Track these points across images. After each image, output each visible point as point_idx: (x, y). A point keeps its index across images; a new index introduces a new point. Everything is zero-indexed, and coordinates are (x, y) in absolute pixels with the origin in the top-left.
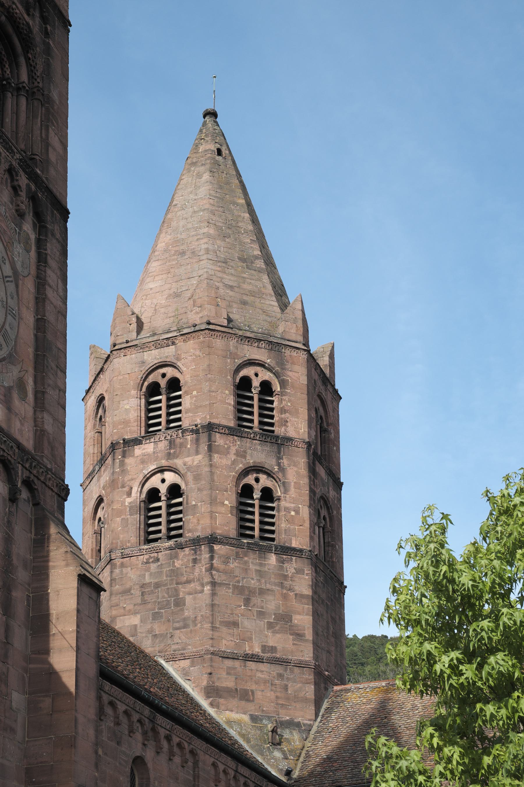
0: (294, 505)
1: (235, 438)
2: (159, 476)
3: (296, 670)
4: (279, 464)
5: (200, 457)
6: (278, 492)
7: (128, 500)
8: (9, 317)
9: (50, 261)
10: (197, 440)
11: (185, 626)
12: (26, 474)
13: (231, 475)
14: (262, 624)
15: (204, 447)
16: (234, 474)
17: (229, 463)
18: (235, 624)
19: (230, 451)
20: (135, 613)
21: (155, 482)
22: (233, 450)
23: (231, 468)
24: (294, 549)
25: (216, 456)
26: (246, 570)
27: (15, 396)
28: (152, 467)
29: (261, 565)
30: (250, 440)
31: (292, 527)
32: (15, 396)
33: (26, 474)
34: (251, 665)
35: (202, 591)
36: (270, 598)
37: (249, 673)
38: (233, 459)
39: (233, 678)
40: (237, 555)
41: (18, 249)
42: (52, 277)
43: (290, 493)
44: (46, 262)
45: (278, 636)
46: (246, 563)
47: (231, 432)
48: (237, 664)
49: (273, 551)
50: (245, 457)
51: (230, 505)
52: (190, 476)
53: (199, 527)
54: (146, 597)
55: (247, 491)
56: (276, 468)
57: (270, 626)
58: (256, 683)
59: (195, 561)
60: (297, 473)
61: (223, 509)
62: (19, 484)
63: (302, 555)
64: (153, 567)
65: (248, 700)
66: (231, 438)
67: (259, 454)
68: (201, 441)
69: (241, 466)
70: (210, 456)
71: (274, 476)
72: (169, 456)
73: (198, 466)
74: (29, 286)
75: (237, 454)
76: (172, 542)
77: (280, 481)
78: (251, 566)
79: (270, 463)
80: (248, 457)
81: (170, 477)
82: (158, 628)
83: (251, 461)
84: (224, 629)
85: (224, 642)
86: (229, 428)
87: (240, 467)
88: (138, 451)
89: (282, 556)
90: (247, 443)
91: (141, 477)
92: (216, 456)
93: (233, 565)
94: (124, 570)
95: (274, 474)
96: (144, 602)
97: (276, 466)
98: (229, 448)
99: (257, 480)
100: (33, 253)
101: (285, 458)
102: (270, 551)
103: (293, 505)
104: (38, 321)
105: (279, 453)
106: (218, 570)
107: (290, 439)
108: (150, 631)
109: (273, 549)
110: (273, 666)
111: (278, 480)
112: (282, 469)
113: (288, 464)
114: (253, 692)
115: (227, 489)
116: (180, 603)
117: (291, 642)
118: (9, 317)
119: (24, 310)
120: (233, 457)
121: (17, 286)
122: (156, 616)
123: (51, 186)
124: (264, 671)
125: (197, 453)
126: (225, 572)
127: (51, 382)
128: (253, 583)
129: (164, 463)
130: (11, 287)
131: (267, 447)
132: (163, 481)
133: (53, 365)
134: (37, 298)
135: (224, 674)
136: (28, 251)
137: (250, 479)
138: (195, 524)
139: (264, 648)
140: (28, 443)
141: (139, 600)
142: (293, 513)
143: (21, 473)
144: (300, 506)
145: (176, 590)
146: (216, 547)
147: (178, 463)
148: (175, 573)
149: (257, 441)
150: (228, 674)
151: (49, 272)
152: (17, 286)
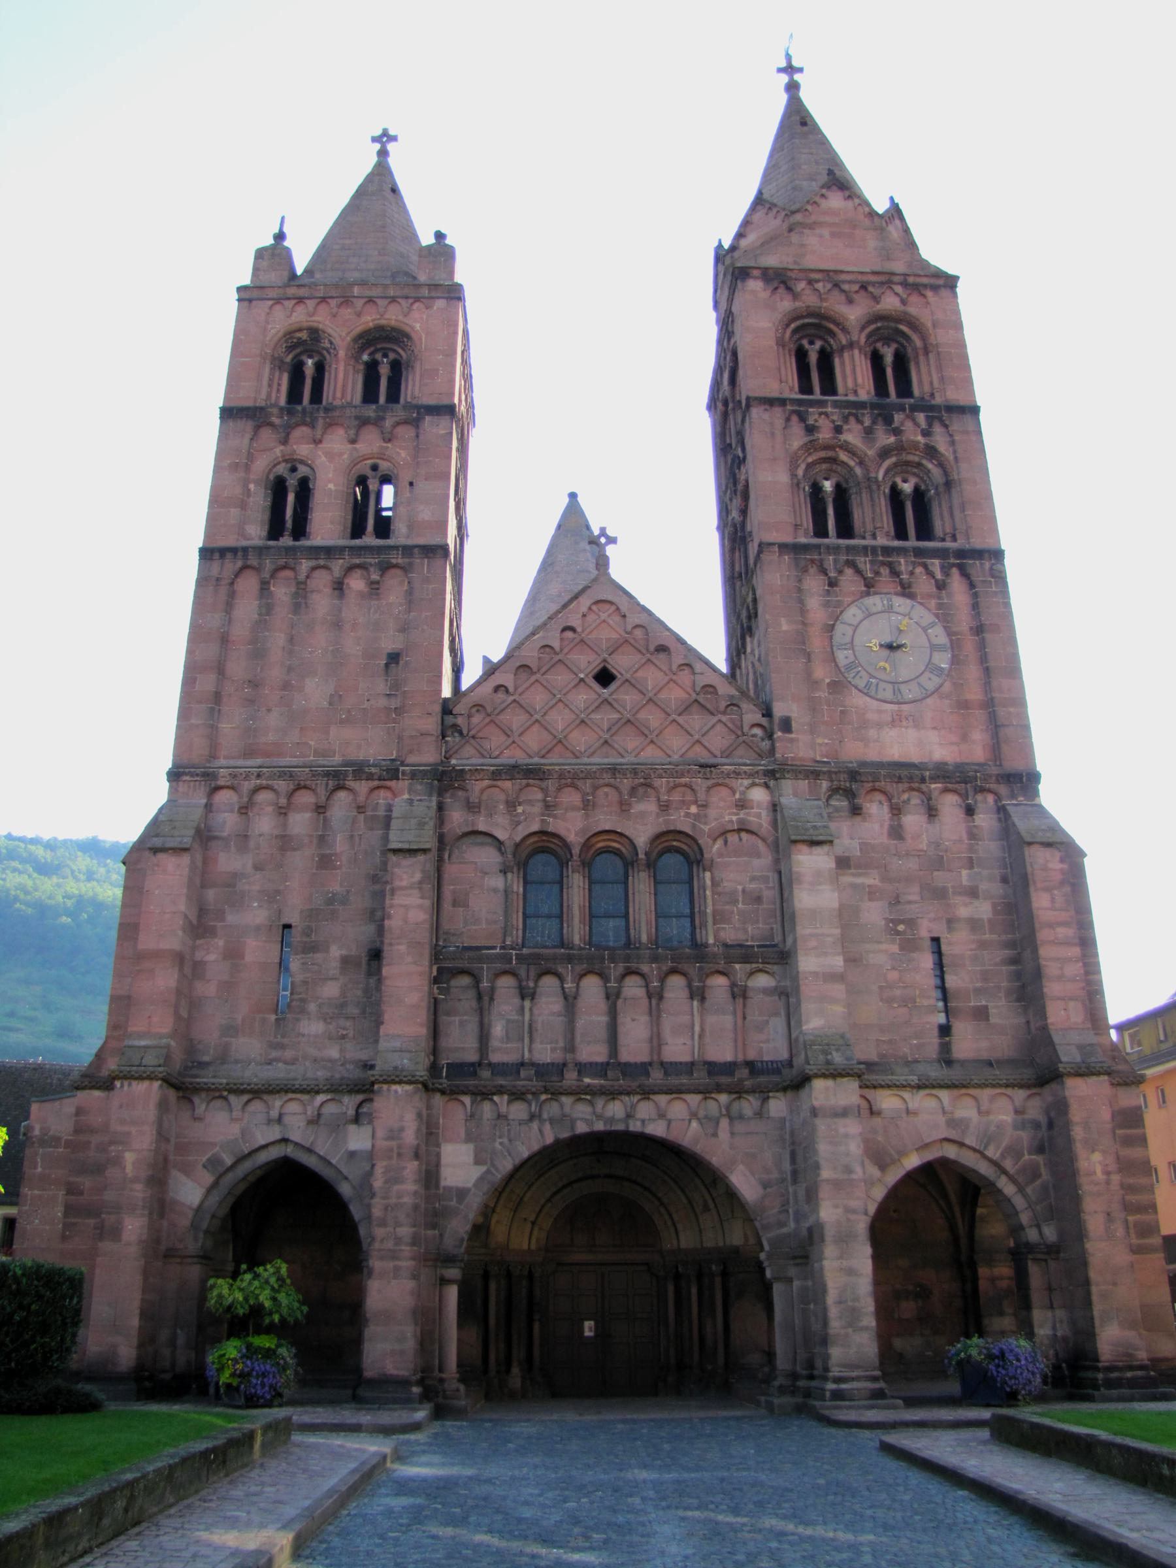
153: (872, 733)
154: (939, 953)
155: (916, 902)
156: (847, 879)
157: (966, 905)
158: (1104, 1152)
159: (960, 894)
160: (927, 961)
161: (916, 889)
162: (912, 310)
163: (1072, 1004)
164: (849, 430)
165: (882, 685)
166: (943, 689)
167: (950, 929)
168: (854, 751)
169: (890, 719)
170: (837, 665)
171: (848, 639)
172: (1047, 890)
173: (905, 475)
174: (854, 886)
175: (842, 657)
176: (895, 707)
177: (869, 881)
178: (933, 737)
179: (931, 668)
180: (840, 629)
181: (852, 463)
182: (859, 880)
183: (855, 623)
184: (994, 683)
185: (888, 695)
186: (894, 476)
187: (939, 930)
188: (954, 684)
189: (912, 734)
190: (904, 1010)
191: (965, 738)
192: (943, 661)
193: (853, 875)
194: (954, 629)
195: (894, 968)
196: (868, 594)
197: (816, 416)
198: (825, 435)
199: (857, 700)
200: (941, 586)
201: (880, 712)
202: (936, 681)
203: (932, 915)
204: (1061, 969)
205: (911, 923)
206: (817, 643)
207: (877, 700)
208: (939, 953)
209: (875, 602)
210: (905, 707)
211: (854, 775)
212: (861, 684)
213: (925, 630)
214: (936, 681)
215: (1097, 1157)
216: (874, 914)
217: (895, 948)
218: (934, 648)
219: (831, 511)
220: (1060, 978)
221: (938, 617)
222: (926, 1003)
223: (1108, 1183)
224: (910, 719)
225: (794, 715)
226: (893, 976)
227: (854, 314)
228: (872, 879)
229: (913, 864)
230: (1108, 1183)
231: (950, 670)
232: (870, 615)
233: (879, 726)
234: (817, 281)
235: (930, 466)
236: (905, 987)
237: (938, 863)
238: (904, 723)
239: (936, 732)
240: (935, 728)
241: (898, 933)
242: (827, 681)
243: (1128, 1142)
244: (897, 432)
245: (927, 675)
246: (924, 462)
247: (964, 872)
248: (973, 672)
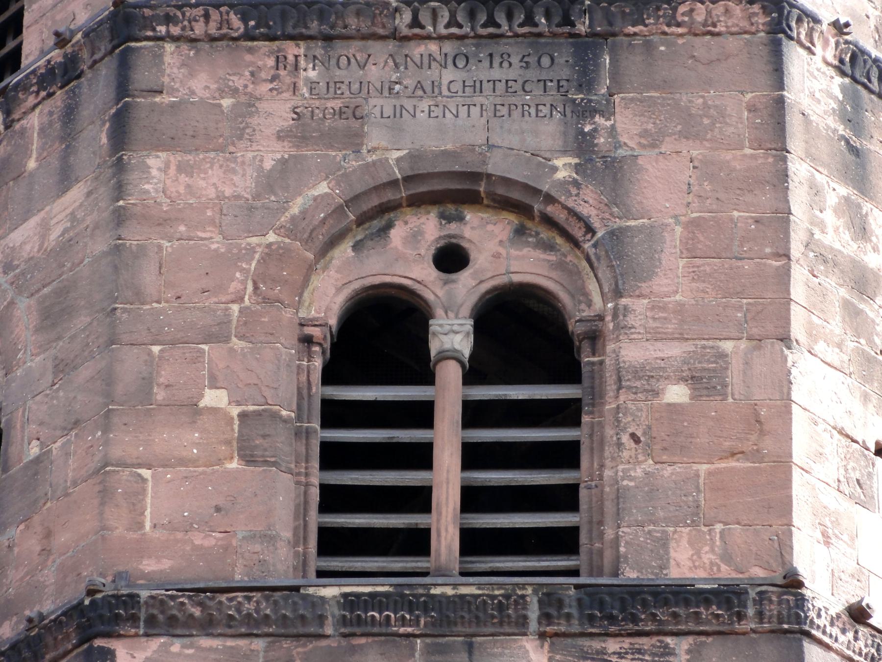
0: (689, 347)
1: (292, 49)
4: (583, 146)
6: (584, 301)
10: (70, 114)
13: (252, 250)
16: (272, 237)
17: (243, 184)
19: (254, 121)
22: (277, 112)
23: (250, 213)
30: (391, 45)
31: (668, 471)
38: (268, 164)
43: (660, 283)
49: (533, 625)
50: (353, 141)
51: (235, 411)
55: (379, 336)
56: (564, 167)
60: (706, 169)
61: (188, 441)
63: (740, 616)
66: (263, 56)
68: (86, 112)
69: (323, 188)
70: (120, 166)
71: (550, 209)
75: (302, 131)
77: (590, 230)
79: (527, 141)
80: (376, 137)
83: (387, 150)
89: (596, 644)
92: (155, 162)
95: (550, 199)
97: (564, 152)
98: (249, 105)
99: (451, 259)
101: (628, 102)
103: (675, 350)
105: (586, 79)
109: (533, 613)
111: (578, 232)
112: (605, 168)
113: (645, 133)
115: (225, 322)
120: (271, 154)
142: (677, 393)
144: (728, 346)
149: (433, 47)
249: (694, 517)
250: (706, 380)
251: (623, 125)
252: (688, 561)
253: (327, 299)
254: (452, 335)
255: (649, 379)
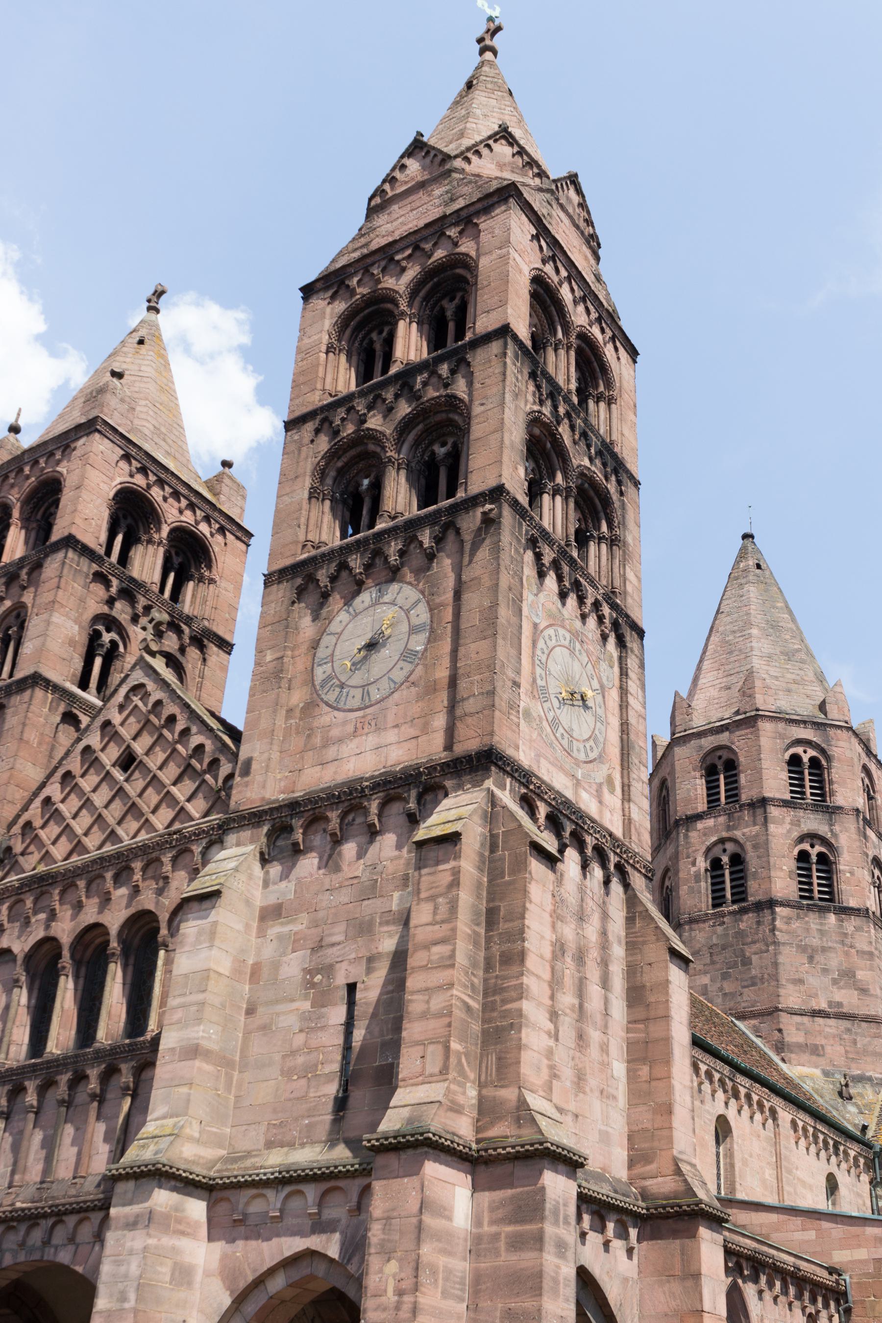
2: (720, 847)
3: (864, 1024)
4: (831, 831)
5: (757, 827)
7: (693, 869)
8: (598, 724)
9: (630, 673)
11: (754, 984)
12: (617, 859)
14: (827, 980)
15: (760, 819)
17: (785, 831)
18: (801, 981)
20: (706, 973)
21: (717, 851)
24: (852, 909)
25: (772, 828)
26: (808, 930)
27: (605, 790)
28: (714, 839)
29: (821, 924)
32: (605, 790)
33: (617, 859)
34: (820, 1021)
35: (767, 951)
36: (832, 955)
37: (817, 1028)
39: (803, 1033)
40: (798, 917)
41: (604, 666)
42: (633, 686)
44: (627, 675)
45: (843, 991)
46: (807, 922)
47: (785, 804)
48: (805, 1019)
50: (799, 826)
52: (748, 846)
53: (761, 892)
54: (715, 958)
55: (803, 856)
57: (835, 982)
58: (825, 1038)
59: (759, 923)
60: (849, 837)
61: (782, 874)
62: (612, 868)
64: (719, 929)
65: (818, 1055)
66: (785, 809)
67: (813, 823)
72: (729, 828)
73: (757, 835)
74: (614, 695)
75: (792, 823)
76: (735, 907)
78: (812, 926)
79: (823, 829)
81: (730, 846)
82: (728, 987)
84: (790, 987)
85: (791, 998)
86: (784, 801)
87: (795, 834)
88: (700, 825)
90: (801, 813)
91: (704, 849)
93: (796, 925)
94: (693, 933)
96: (713, 962)
100: (616, 669)
102: (829, 911)
104: (622, 724)
106: (781, 931)
107: (840, 808)
108: (721, 989)
110: (840, 1021)
112: (835, 835)
114: (822, 1046)
116: (746, 962)
117: (856, 997)
118: (598, 724)
119: (609, 715)
121: (604, 697)
122: (725, 976)
123: (629, 612)
124: (831, 1026)
125: (755, 824)
126: (788, 932)
127: (635, 776)
128: (815, 942)
129: (725, 834)
130: (600, 697)
131: (820, 816)
132: (725, 851)
133: (636, 761)
134: (621, 706)
135: (793, 1030)
136: (612, 667)
137: (806, 846)
138: (755, 891)
139: (830, 1004)
140: (618, 832)
141: (708, 961)
142: (848, 875)
143: (613, 859)
145: (742, 950)
146: (778, 909)
147: (738, 834)
148: (740, 934)
150: (798, 1029)
151: (630, 683)
152: (604, 697)
153: (331, 752)
154: (351, 1003)
155: (339, 944)
156: (275, 929)
157: (390, 936)
158: (400, 1260)
159: (387, 923)
160: (338, 1014)
161: (341, 928)
162: (462, 249)
163: (431, 1048)
164: (374, 415)
165: (353, 692)
166: (411, 679)
167: (369, 971)
168: (316, 777)
169: (352, 729)
170: (313, 685)
171: (329, 651)
172: (432, 898)
173: (442, 439)
174: (280, 937)
175: (320, 673)
176: (360, 714)
177: (296, 927)
178: (391, 736)
179: (407, 655)
180: (326, 640)
181: (378, 450)
182: (286, 929)
183: (339, 630)
184: (462, 651)
185: (356, 703)
186: (431, 443)
187: (356, 973)
188: (425, 666)
189: (371, 740)
190: (303, 1082)
191: (426, 729)
192: (418, 644)
193: (282, 924)
194: (437, 601)
195: (301, 1031)
196: (358, 592)
197: (343, 415)
198: (350, 429)
199: (326, 717)
200: (431, 557)
201: (345, 723)
202: (408, 667)
203: (353, 956)
204: (428, 1002)
205: (328, 970)
206: (296, 666)
207: (344, 711)
208: (351, 1003)
209: (365, 598)
210: (368, 711)
211: (293, 806)
212: (331, 697)
213: (407, 612)
214: (408, 667)
215: (392, 1267)
216: (293, 966)
217: (307, 1005)
218: (414, 630)
219: (364, 512)
220: (425, 1015)
221: (422, 593)
222: (327, 1070)
223: (398, 1307)
224: (373, 724)
225: (255, 755)
226: (299, 1040)
227: (399, 284)
228: (300, 925)
229: (344, 896)
230: (398, 1307)
231: (426, 650)
232: (357, 615)
233: (340, 740)
234: (373, 264)
235: (456, 417)
236: (308, 1053)
237: (371, 890)
238: (366, 730)
239: (396, 730)
240: (397, 726)
241: (313, 985)
242: (301, 705)
243: (517, 1243)
244: (414, 396)
245: (401, 664)
246: (451, 416)
247: (396, 895)
248: (446, 646)
249: (852, 896)
250: (852, 873)
251: (837, 828)
252: (852, 903)
253: (796, 852)
254: (814, 858)
255: (844, 871)
